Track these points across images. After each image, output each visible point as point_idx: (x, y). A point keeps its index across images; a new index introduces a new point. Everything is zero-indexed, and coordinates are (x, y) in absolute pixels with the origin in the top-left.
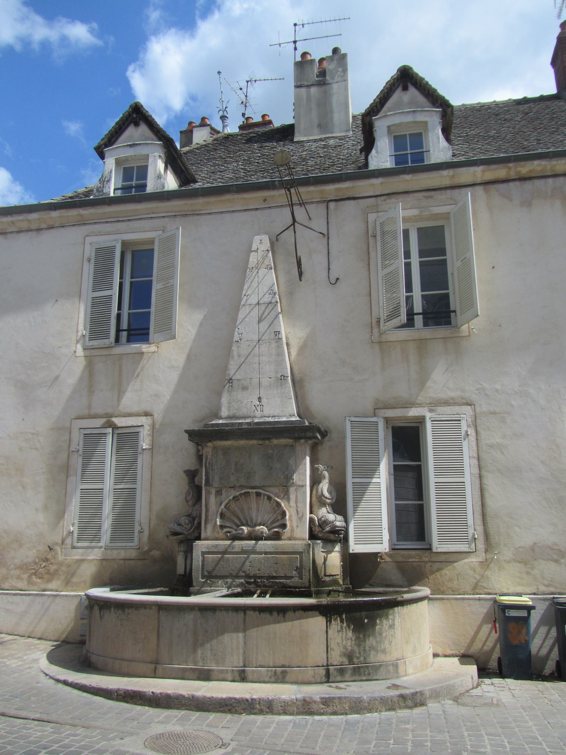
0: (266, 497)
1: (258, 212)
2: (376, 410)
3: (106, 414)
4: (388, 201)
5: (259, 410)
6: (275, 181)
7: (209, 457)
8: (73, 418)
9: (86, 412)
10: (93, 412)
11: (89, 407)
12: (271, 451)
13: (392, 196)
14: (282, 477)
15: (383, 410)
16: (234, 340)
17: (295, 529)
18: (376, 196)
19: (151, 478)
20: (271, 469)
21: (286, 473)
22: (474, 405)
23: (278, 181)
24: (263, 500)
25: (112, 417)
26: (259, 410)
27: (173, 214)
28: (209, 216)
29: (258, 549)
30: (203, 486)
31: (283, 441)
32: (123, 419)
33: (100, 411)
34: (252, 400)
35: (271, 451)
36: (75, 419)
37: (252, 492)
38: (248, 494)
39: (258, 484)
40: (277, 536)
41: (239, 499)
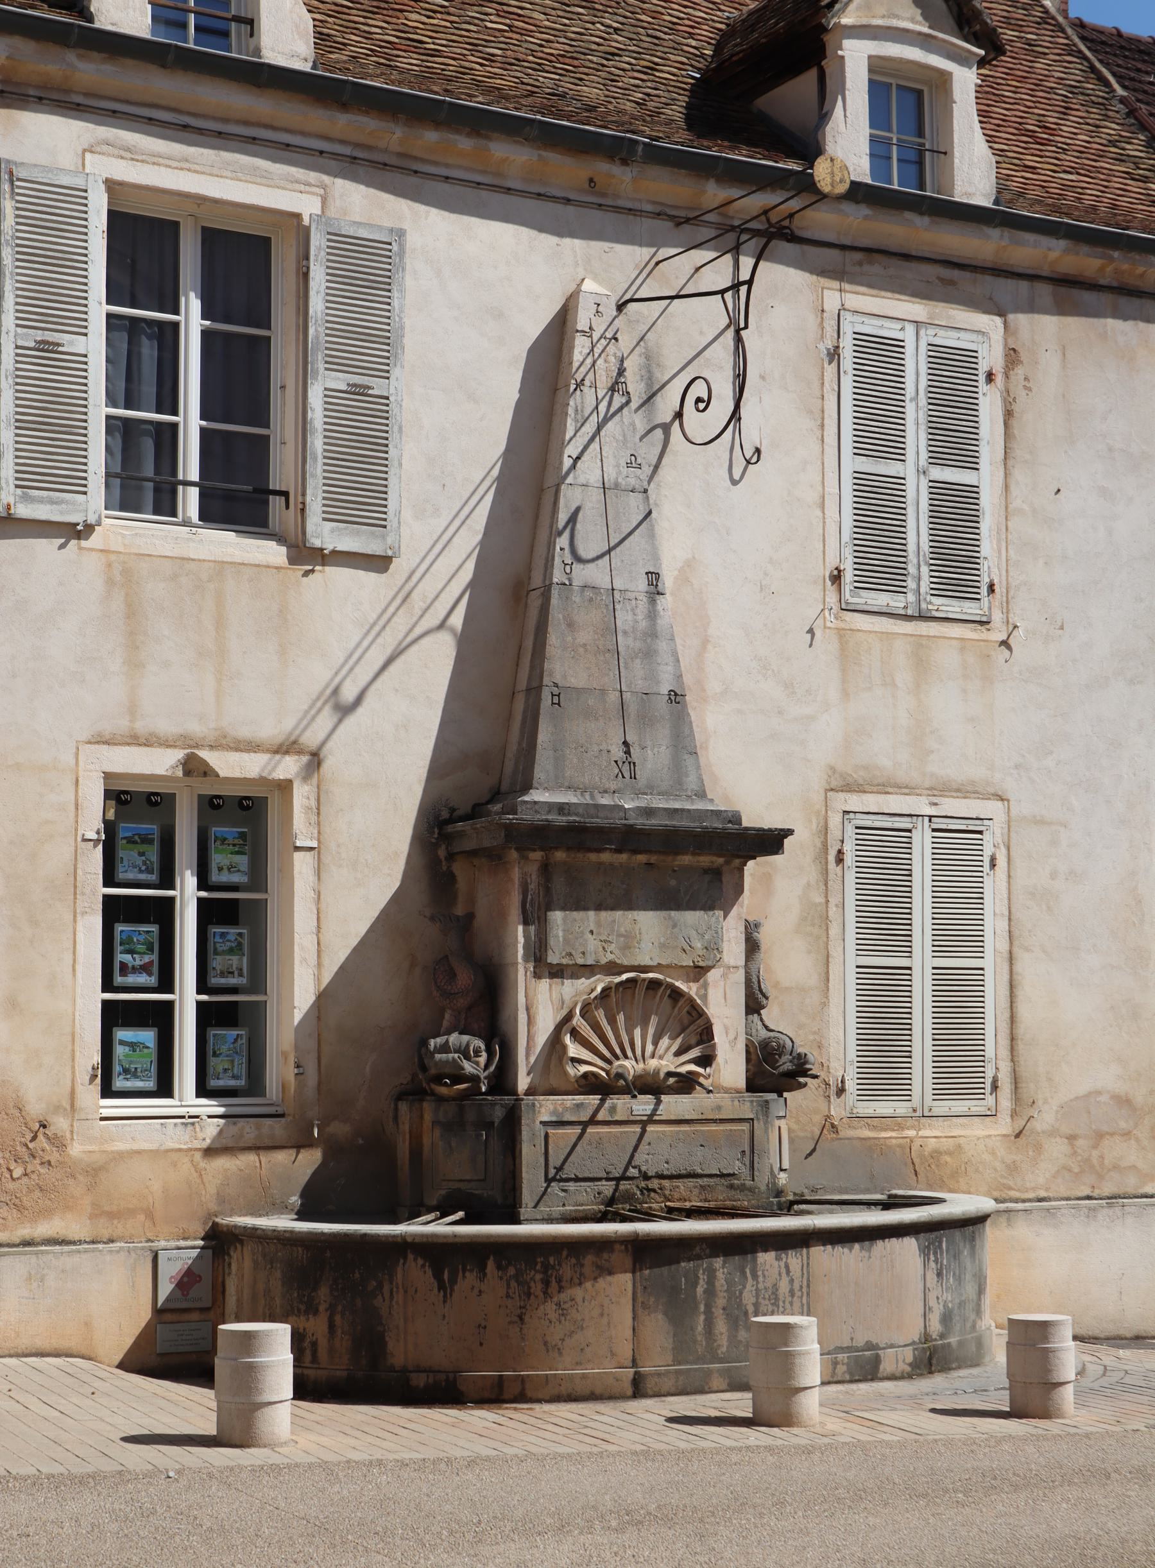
1: (570, 209)
2: (830, 794)
3: (184, 737)
4: (866, 268)
5: (627, 775)
6: (637, 142)
7: (531, 887)
8: (84, 738)
9: (122, 725)
10: (141, 727)
11: (132, 710)
12: (673, 883)
14: (699, 945)
15: (841, 795)
16: (555, 580)
18: (843, 247)
19: (319, 927)
20: (674, 926)
22: (1008, 801)
23: (644, 143)
24: (661, 998)
25: (197, 746)
26: (627, 775)
27: (347, 150)
28: (446, 187)
29: (664, 1112)
30: (520, 960)
31: (705, 860)
32: (234, 757)
33: (165, 727)
34: (610, 748)
35: (673, 883)
36: (90, 743)
37: (644, 980)
39: (646, 961)
40: (686, 1084)
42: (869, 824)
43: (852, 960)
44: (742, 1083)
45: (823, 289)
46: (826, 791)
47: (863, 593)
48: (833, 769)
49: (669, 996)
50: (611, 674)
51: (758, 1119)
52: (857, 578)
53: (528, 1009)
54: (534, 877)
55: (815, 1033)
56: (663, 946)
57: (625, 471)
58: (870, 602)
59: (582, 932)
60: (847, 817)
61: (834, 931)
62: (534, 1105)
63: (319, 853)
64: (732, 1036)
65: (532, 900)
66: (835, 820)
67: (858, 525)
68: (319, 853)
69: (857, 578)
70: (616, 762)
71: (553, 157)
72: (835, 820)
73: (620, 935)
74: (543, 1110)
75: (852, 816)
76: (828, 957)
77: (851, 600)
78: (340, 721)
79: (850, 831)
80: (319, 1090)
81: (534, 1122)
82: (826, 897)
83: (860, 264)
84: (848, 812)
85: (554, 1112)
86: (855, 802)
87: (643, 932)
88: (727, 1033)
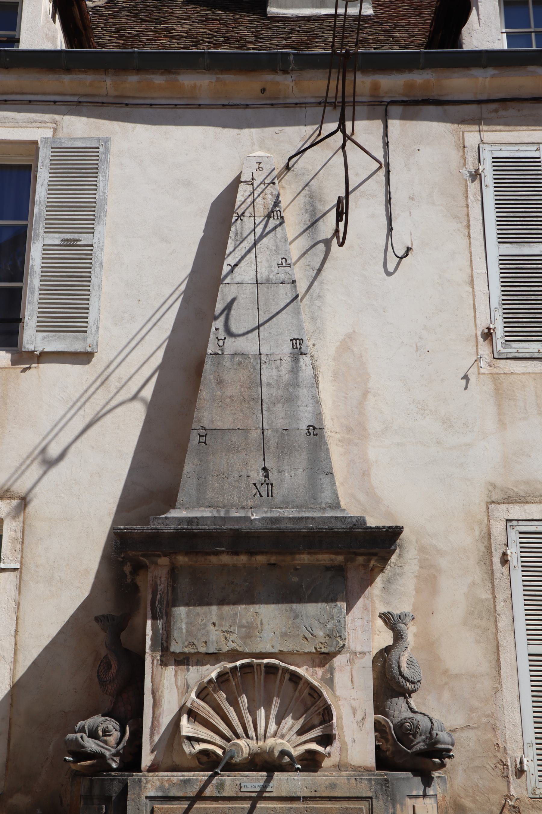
0: (287, 676)
1: (249, 111)
2: (490, 506)
4: (501, 113)
5: (264, 494)
6: (288, 54)
7: (161, 587)
12: (295, 579)
13: (509, 103)
14: (321, 633)
15: (504, 507)
16: (209, 351)
17: (349, 746)
18: (479, 102)
19: (17, 631)
20: (296, 617)
21: (329, 626)
23: (294, 54)
24: (281, 682)
26: (264, 494)
27: (76, 99)
28: (150, 110)
30: (147, 650)
31: (324, 558)
34: (249, 473)
35: (295, 579)
37: (259, 665)
38: (247, 670)
39: (268, 649)
40: (311, 762)
41: (228, 680)
42: (533, 529)
43: (524, 649)
44: (371, 761)
45: (463, 132)
46: (488, 503)
47: (513, 344)
48: (494, 486)
49: (290, 679)
50: (255, 416)
51: (377, 798)
52: (507, 334)
53: (153, 693)
54: (163, 579)
55: (488, 716)
56: (284, 635)
57: (276, 270)
58: (520, 350)
59: (205, 625)
60: (509, 524)
61: (503, 622)
62: (140, 781)
63: (21, 573)
64: (359, 717)
65: (161, 598)
66: (498, 528)
67: (505, 294)
68: (21, 573)
69: (507, 334)
70: (255, 484)
71: (228, 78)
72: (498, 528)
73: (241, 626)
74: (149, 786)
75: (515, 523)
76: (498, 646)
77: (503, 351)
78: (45, 473)
79: (514, 536)
80: (7, 766)
81: (139, 797)
82: (493, 593)
83: (496, 111)
84: (511, 520)
85: (161, 788)
86: (517, 511)
87: (264, 622)
88: (354, 714)
